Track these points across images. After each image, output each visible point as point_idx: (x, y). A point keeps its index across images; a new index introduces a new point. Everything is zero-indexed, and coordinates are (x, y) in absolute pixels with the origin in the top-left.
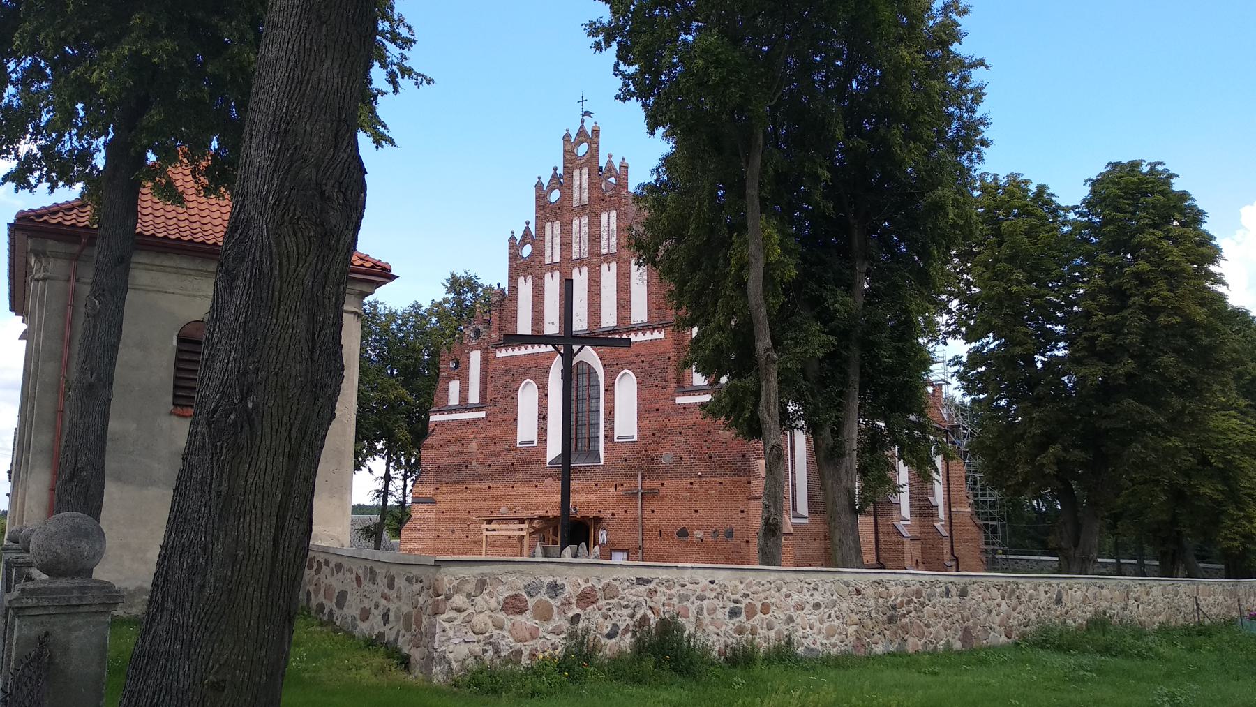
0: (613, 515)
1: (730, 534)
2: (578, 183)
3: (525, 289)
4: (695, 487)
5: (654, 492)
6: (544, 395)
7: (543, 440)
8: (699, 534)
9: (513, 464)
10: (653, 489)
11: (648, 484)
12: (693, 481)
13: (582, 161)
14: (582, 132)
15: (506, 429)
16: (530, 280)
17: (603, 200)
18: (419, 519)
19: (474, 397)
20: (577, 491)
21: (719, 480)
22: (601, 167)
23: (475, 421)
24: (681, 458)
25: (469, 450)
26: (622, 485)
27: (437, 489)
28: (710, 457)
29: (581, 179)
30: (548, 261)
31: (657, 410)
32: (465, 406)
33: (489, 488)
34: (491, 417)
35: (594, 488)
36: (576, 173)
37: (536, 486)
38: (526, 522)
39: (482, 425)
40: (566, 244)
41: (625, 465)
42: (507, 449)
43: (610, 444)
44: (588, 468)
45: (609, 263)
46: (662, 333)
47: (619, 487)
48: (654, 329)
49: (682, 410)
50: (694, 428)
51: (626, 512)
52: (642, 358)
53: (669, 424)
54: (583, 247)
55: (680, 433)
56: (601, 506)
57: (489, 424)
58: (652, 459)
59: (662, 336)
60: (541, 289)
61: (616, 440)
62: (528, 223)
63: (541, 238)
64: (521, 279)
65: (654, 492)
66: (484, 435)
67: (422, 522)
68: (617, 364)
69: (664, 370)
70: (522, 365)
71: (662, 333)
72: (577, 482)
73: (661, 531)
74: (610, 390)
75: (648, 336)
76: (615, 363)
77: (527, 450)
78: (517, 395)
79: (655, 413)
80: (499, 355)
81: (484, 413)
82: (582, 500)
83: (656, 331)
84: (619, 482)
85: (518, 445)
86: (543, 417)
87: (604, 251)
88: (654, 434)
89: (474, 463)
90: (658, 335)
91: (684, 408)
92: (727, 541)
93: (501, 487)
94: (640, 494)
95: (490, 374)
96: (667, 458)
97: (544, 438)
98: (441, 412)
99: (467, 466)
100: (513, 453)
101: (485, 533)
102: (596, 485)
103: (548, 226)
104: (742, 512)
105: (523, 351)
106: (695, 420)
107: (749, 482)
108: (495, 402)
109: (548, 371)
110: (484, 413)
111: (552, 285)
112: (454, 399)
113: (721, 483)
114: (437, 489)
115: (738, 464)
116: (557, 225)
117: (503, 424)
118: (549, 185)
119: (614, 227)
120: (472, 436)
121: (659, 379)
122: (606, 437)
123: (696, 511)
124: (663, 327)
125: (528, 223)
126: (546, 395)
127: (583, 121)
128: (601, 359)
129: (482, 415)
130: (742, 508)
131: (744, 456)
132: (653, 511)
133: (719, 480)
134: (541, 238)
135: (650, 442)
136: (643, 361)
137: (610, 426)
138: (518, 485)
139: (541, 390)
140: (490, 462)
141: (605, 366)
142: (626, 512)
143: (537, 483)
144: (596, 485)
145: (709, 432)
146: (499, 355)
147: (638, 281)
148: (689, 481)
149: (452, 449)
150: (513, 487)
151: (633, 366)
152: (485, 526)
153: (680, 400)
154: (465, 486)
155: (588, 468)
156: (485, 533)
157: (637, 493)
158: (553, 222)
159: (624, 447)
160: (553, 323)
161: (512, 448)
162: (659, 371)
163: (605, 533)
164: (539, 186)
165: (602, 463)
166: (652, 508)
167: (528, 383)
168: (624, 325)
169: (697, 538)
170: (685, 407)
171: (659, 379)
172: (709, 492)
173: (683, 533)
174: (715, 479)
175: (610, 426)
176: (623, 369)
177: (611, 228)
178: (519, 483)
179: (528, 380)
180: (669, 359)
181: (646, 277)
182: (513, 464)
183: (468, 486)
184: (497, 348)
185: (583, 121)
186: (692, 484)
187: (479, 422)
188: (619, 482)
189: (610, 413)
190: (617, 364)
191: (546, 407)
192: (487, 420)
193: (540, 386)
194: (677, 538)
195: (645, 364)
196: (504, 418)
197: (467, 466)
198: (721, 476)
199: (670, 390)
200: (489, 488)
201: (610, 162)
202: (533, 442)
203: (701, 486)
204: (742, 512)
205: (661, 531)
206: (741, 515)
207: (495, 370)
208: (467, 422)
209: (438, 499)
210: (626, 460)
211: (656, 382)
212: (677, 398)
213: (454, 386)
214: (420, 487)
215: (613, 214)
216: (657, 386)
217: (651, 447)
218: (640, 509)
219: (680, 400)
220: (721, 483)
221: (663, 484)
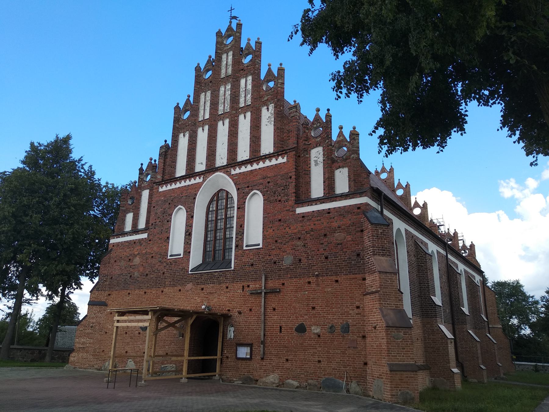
0: (240, 313)
1: (346, 329)
2: (225, 62)
3: (184, 141)
4: (313, 286)
5: (274, 292)
6: (190, 217)
7: (187, 252)
8: (316, 330)
9: (164, 273)
10: (273, 289)
11: (271, 284)
12: (310, 280)
13: (228, 47)
14: (230, 29)
15: (161, 245)
16: (187, 135)
17: (242, 70)
18: (93, 318)
20: (211, 293)
21: (334, 278)
22: (242, 48)
23: (140, 241)
24: (300, 260)
25: (134, 264)
26: (248, 286)
27: (109, 295)
28: (326, 258)
29: (228, 59)
30: (201, 119)
31: (280, 220)
32: (135, 231)
33: (145, 293)
34: (151, 237)
35: (225, 290)
36: (224, 56)
37: (180, 290)
38: (150, 313)
39: (144, 244)
40: (214, 105)
41: (251, 269)
42: (160, 261)
43: (240, 251)
44: (221, 273)
45: (245, 113)
46: (285, 158)
47: (246, 289)
48: (278, 155)
49: (301, 219)
50: (312, 233)
52: (269, 180)
53: (290, 232)
54: (226, 105)
55: (299, 238)
56: (230, 305)
57: (149, 242)
58: (275, 263)
59: (285, 160)
60: (194, 139)
61: (245, 248)
62: (189, 96)
63: (197, 104)
64: (181, 135)
65: (274, 292)
66: (145, 251)
67: (94, 321)
69: (286, 187)
70: (176, 195)
71: (285, 158)
72: (211, 285)
73: (281, 327)
74: (241, 208)
75: (274, 162)
76: (247, 185)
77: (175, 261)
78: (171, 218)
79: (277, 223)
80: (161, 190)
81: (147, 234)
82: (215, 300)
83: (280, 157)
84: (245, 284)
85: (169, 258)
86: (188, 234)
87: (242, 104)
88: (276, 241)
89: (136, 274)
90: (281, 160)
91: (303, 217)
92: (343, 336)
93: (153, 292)
94: (263, 294)
95: (153, 205)
96: (288, 260)
97: (188, 251)
98: (118, 236)
99: (131, 276)
100: (165, 264)
101: (116, 324)
102: (227, 288)
103: (202, 96)
104: (358, 307)
105: (178, 185)
106: (313, 226)
107: (364, 279)
108: (155, 225)
109: (195, 198)
110: (147, 234)
111: (203, 135)
112: (128, 227)
113: (337, 281)
114: (109, 295)
115: (353, 262)
116: (209, 94)
117: (159, 242)
118: (205, 68)
119: (249, 87)
120: (137, 253)
121: (282, 195)
122: (237, 246)
123: (313, 308)
124: (286, 153)
125: (189, 96)
126: (192, 217)
127: (231, 22)
128: (235, 184)
129: (145, 236)
130: (357, 303)
131: (358, 255)
132: (274, 309)
133: (334, 278)
134: (197, 104)
135: (273, 247)
136: (269, 182)
137: (240, 237)
138: (166, 290)
140: (147, 272)
141: (238, 189)
142: (251, 310)
144: (227, 288)
145: (325, 235)
146: (161, 190)
147: (267, 123)
148: (307, 280)
149: (123, 263)
150: (162, 292)
151: (261, 187)
152: (117, 318)
153: (300, 210)
154: (129, 292)
155: (221, 273)
156: (116, 324)
157: (261, 293)
158: (205, 92)
159: (251, 254)
160: (202, 163)
161: (165, 260)
162: (282, 188)
163: (232, 329)
164: (198, 69)
165: (233, 268)
166: (274, 306)
169: (314, 334)
170: (303, 216)
171: (282, 195)
172: (326, 290)
173: (301, 329)
174: (332, 277)
175: (240, 237)
176: (252, 190)
177: (247, 88)
178: (167, 288)
179: (180, 206)
180: (291, 177)
181: (273, 119)
182: (164, 273)
183: (130, 292)
184: (159, 185)
185: (231, 22)
186: (309, 283)
187: (142, 242)
188: (245, 284)
189: (241, 226)
190: (248, 187)
191: (191, 226)
192: (149, 240)
193: (189, 210)
194: (295, 334)
195: (270, 184)
196: (160, 238)
197: (131, 276)
198: (337, 275)
201: (248, 44)
202: (180, 255)
203: (318, 285)
204: (358, 307)
205: (281, 327)
206: (356, 311)
207: (157, 201)
208: (134, 242)
209: (109, 302)
210: (252, 265)
213: (129, 217)
214: (97, 293)
215: (250, 78)
216: (280, 201)
217: (274, 252)
218: (263, 309)
219: (300, 210)
220: (337, 281)
221: (283, 284)
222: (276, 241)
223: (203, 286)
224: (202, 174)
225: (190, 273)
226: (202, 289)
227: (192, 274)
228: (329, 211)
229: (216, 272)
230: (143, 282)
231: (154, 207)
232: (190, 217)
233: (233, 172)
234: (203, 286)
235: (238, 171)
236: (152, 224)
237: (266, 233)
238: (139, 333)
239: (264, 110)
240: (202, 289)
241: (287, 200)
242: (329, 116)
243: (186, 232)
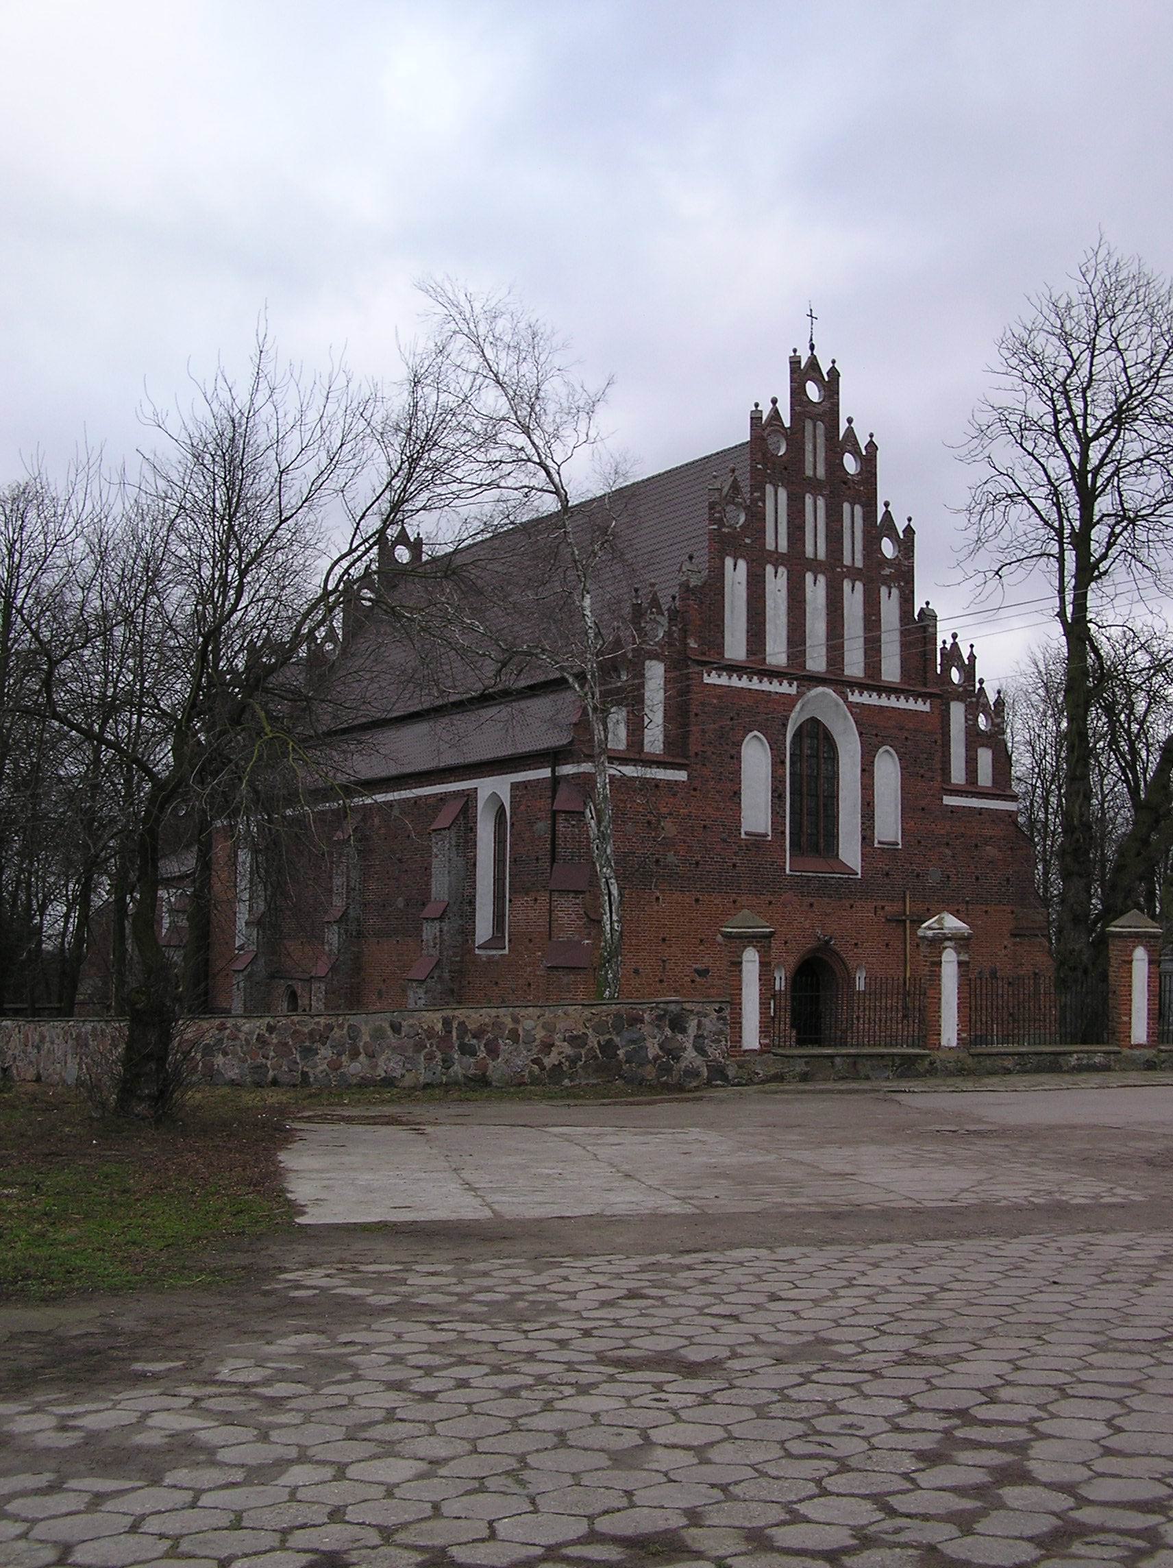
9: (734, 866)
15: (722, 805)
17: (845, 483)
19: (654, 738)
26: (883, 908)
31: (923, 809)
32: (635, 754)
33: (697, 900)
37: (770, 903)
44: (841, 882)
49: (950, 815)
51: (887, 945)
57: (693, 793)
68: (877, 735)
74: (867, 770)
76: (874, 733)
78: (739, 753)
80: (707, 680)
88: (919, 842)
91: (952, 812)
93: (716, 902)
97: (781, 829)
109: (785, 725)
113: (986, 912)
116: (783, 494)
121: (926, 768)
128: (856, 722)
129: (682, 776)
136: (906, 738)
137: (868, 823)
138: (743, 900)
139: (774, 752)
142: (887, 945)
143: (772, 898)
150: (734, 902)
155: (841, 882)
162: (925, 756)
165: (859, 877)
167: (755, 736)
168: (872, 682)
170: (954, 810)
174: (982, 906)
175: (868, 823)
178: (744, 897)
180: (936, 742)
189: (868, 804)
190: (877, 735)
192: (690, 787)
195: (909, 743)
197: (657, 861)
199: (936, 784)
200: (697, 900)
210: (887, 874)
211: (922, 771)
212: (944, 797)
216: (922, 776)
222: (919, 842)
223: (812, 900)
224: (796, 679)
225: (788, 871)
226: (811, 905)
227: (791, 876)
228: (980, 811)
229: (833, 878)
230: (689, 878)
231: (696, 715)
232: (778, 763)
233: (851, 699)
234: (812, 900)
235: (855, 698)
236: (697, 754)
237: (906, 826)
238: (693, 981)
239: (884, 591)
240: (811, 905)
241: (932, 779)
242: (972, 657)
243: (773, 791)
